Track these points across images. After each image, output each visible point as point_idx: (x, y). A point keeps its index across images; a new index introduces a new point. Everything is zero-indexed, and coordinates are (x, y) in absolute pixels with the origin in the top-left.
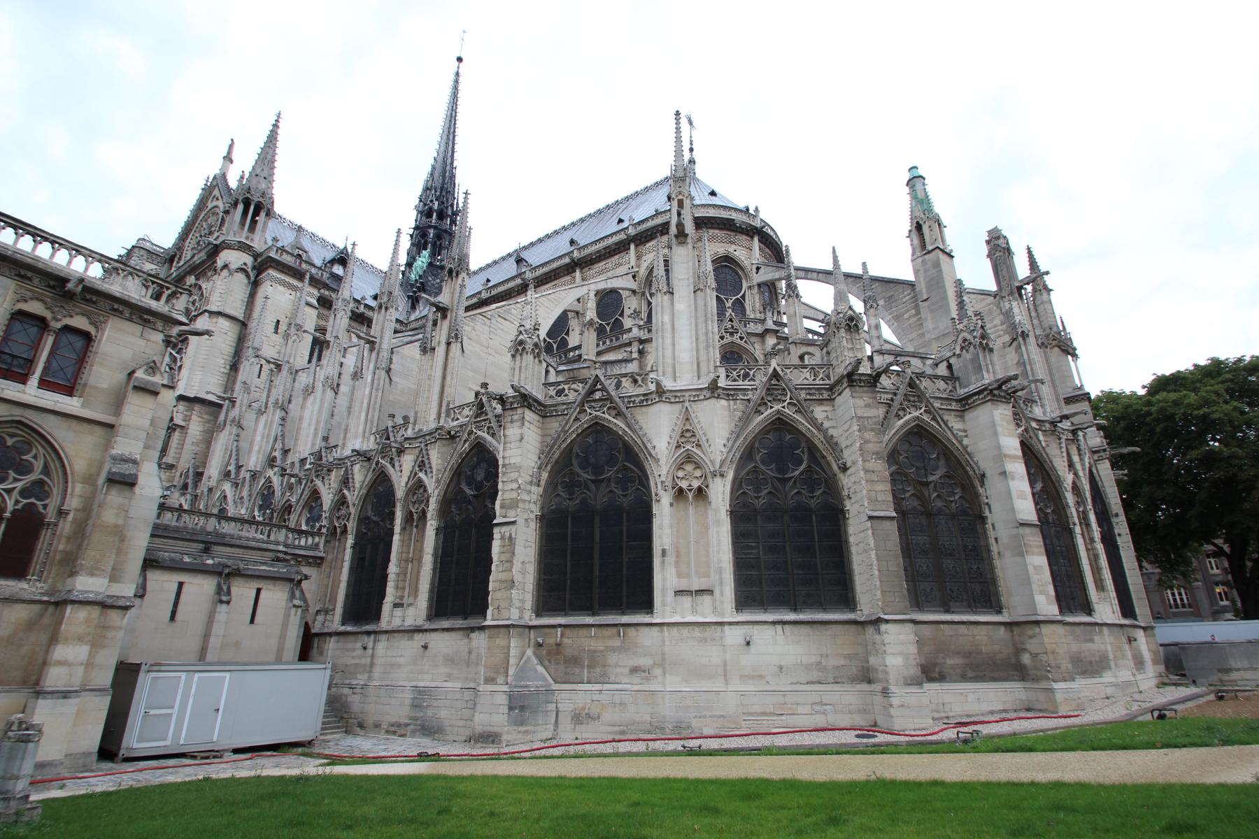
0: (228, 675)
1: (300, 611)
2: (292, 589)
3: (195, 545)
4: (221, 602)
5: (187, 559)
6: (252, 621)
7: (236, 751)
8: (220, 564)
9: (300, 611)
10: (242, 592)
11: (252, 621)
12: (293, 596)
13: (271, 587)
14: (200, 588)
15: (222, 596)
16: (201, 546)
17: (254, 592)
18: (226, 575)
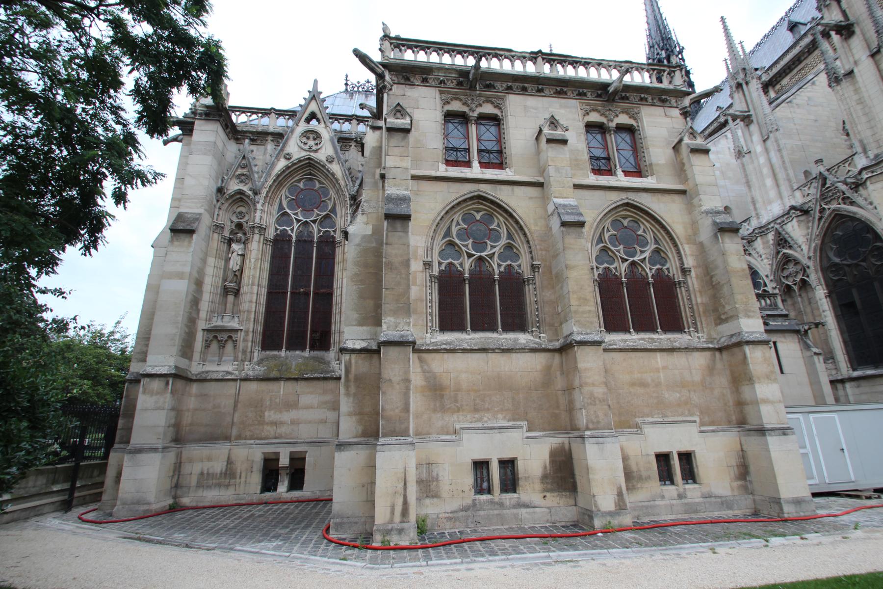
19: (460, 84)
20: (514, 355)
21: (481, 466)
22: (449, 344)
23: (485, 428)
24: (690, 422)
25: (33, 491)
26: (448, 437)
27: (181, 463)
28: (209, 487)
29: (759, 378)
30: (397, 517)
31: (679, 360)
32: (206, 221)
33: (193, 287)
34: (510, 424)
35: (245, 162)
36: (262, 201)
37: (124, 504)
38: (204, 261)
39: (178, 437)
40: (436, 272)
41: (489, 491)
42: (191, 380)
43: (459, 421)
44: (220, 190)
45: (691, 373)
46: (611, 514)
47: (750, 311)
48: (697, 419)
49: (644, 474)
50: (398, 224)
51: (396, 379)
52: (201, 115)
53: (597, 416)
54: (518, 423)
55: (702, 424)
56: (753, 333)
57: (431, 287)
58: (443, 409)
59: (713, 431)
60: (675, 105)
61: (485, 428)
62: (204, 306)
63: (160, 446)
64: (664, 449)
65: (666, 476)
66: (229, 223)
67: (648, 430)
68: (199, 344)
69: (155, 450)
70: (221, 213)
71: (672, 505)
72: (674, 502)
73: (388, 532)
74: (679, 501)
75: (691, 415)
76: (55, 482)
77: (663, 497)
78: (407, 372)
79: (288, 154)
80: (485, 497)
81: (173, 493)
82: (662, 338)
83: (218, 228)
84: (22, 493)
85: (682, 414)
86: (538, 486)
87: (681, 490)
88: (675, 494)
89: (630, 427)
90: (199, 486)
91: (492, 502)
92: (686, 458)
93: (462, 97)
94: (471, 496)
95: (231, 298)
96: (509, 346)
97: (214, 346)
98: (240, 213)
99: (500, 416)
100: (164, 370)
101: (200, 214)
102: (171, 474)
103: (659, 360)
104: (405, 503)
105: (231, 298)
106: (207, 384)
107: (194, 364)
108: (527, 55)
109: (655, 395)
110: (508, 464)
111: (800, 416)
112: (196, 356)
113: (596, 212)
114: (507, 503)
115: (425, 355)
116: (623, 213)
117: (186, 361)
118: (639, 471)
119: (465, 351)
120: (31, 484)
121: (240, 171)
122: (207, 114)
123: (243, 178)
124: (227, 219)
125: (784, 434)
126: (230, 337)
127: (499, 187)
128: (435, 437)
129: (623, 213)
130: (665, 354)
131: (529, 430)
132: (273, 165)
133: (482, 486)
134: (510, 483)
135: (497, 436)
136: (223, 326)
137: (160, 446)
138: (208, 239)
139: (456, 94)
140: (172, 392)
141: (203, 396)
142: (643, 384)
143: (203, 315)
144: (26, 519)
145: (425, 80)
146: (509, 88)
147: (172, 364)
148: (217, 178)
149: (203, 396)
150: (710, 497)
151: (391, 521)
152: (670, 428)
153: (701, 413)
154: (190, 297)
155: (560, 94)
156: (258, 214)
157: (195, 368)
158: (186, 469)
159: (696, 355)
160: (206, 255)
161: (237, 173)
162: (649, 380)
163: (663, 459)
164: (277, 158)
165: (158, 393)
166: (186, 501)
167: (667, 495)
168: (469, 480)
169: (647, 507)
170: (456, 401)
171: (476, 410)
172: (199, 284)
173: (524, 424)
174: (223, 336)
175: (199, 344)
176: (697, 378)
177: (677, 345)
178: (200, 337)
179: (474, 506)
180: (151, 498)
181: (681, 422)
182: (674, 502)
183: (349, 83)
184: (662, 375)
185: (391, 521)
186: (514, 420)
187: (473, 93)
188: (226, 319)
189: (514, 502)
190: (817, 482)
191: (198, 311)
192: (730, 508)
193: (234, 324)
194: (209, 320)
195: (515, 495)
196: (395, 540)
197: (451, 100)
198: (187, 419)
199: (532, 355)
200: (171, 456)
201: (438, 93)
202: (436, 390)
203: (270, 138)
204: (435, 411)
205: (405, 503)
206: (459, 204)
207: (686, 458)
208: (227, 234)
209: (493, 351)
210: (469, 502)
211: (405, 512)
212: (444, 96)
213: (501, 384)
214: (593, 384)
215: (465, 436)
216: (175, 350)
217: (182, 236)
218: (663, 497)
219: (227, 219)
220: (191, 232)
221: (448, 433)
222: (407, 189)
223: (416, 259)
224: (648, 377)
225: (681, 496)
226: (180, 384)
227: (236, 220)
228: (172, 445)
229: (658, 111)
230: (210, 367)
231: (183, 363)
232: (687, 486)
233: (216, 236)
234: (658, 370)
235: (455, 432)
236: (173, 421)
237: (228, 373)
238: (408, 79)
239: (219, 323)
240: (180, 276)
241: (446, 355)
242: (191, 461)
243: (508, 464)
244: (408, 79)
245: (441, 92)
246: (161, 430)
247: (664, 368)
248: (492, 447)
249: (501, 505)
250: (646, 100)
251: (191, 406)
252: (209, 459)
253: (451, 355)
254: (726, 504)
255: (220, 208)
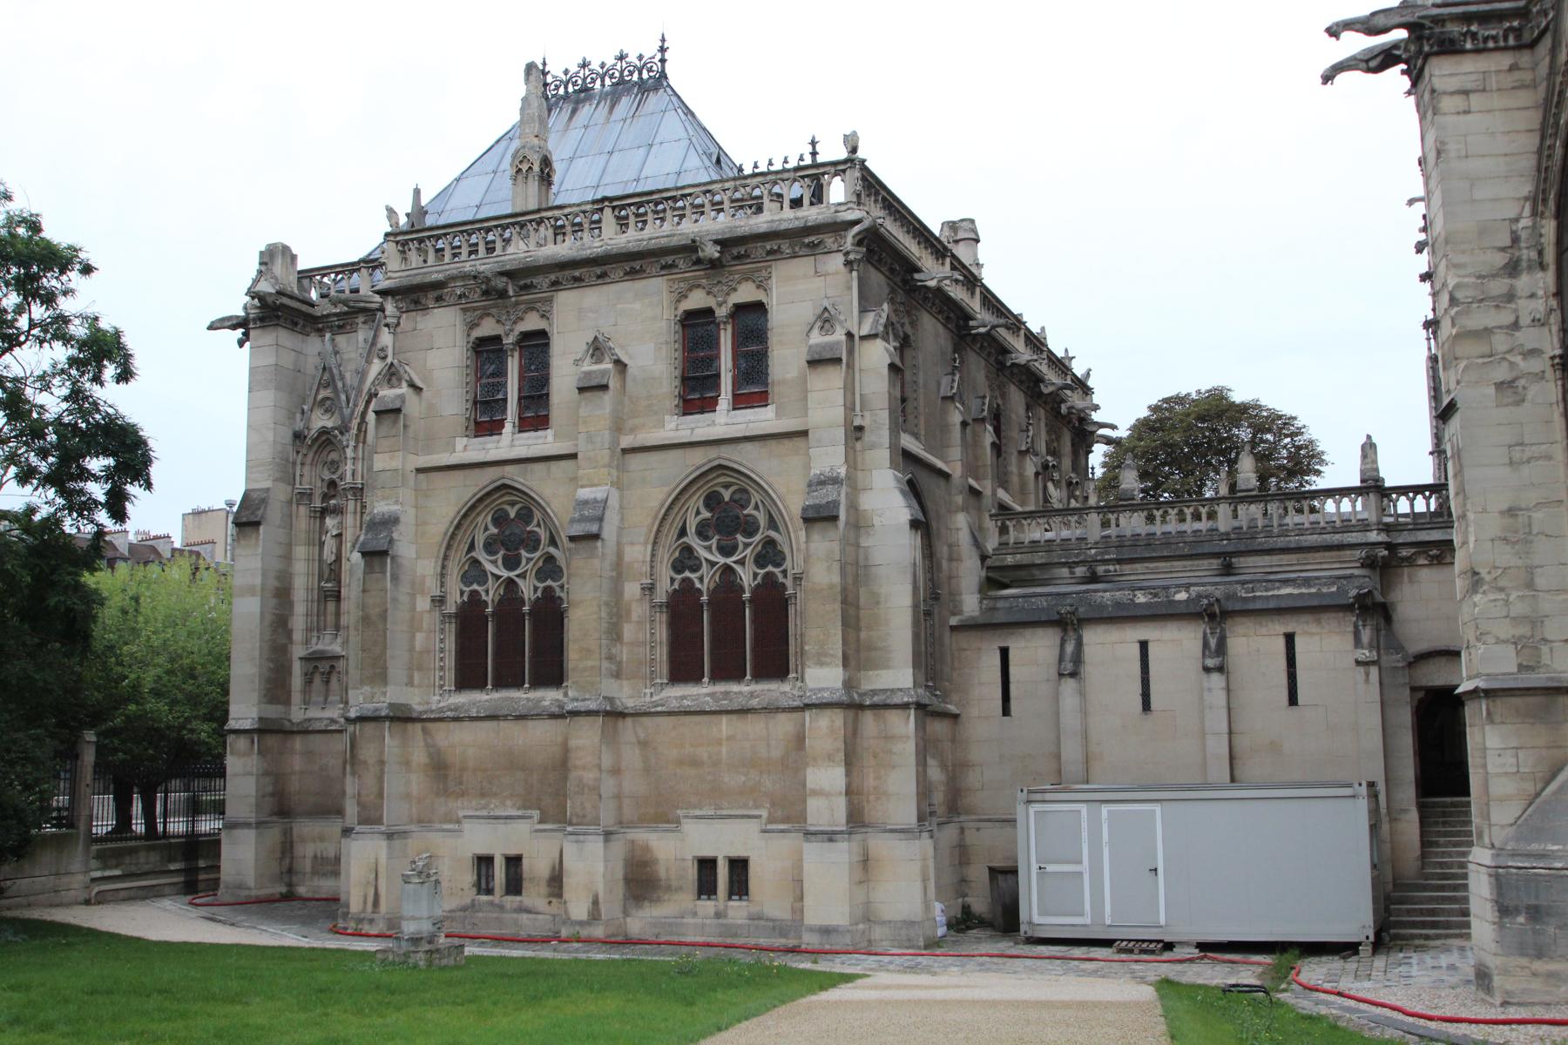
0: (1157, 808)
1: (1374, 671)
2: (1356, 627)
3: (1205, 563)
4: (1207, 670)
5: (1141, 598)
6: (1293, 700)
7: (1204, 947)
8: (1199, 596)
9: (1374, 671)
10: (1255, 646)
11: (1293, 700)
12: (1358, 643)
13: (1314, 628)
14: (1177, 645)
15: (1217, 660)
16: (1216, 563)
17: (1281, 643)
18: (1215, 616)
19: (486, 293)
20: (530, 723)
21: (484, 862)
22: (456, 709)
23: (489, 817)
24: (749, 817)
25: (146, 868)
26: (450, 826)
27: (292, 843)
28: (324, 875)
29: (815, 759)
30: (369, 908)
31: (755, 727)
32: (281, 493)
33: (273, 602)
34: (520, 813)
35: (328, 377)
36: (352, 443)
37: (227, 887)
38: (288, 557)
39: (281, 807)
40: (451, 608)
41: (489, 891)
42: (292, 732)
43: (462, 808)
44: (298, 436)
45: (769, 745)
46: (581, 923)
47: (826, 655)
48: (764, 813)
49: (674, 884)
50: (376, 561)
51: (371, 761)
52: (254, 320)
53: (583, 808)
54: (529, 812)
55: (771, 820)
56: (821, 690)
57: (442, 631)
58: (445, 792)
59: (782, 831)
60: (835, 247)
61: (489, 817)
62: (298, 623)
63: (253, 820)
64: (707, 853)
65: (706, 887)
66: (319, 484)
67: (689, 827)
68: (297, 681)
69: (247, 825)
70: (307, 468)
71: (703, 925)
72: (708, 921)
73: (360, 921)
74: (715, 921)
75: (756, 807)
76: (171, 860)
77: (695, 914)
78: (382, 752)
79: (382, 350)
80: (484, 898)
81: (286, 880)
82: (744, 690)
83: (306, 496)
84: (133, 869)
85: (745, 806)
86: (544, 889)
87: (722, 907)
88: (712, 911)
89: (668, 822)
90: (315, 873)
91: (491, 903)
92: (739, 866)
93: (493, 311)
94: (470, 894)
95: (331, 606)
96: (524, 712)
97: (317, 680)
98: (333, 462)
99: (509, 803)
100: (247, 725)
101: (268, 490)
102: (278, 855)
103: (724, 727)
104: (376, 894)
105: (331, 606)
106: (311, 737)
107: (294, 708)
108: (588, 207)
109: (709, 778)
110: (514, 862)
111: (1083, 808)
112: (296, 697)
113: (666, 489)
114: (508, 906)
115: (429, 725)
116: (722, 480)
117: (280, 708)
118: (668, 879)
119: (472, 719)
120: (142, 860)
121: (323, 394)
122: (262, 319)
123: (328, 403)
124: (312, 478)
125: (831, 840)
126: (332, 667)
127: (530, 466)
128: (437, 826)
129: (722, 480)
130: (734, 717)
131: (541, 822)
132: (362, 374)
133: (484, 885)
134: (515, 885)
135: (501, 827)
136: (323, 652)
137: (253, 820)
138: (288, 522)
139: (485, 308)
140: (260, 752)
141: (309, 754)
142: (695, 763)
143: (298, 636)
144: (144, 898)
145: (439, 299)
146: (555, 283)
147: (255, 715)
148: (291, 416)
149: (309, 754)
150: (760, 918)
151: (364, 910)
152: (718, 825)
153: (773, 804)
154: (269, 618)
155: (633, 274)
156: (349, 467)
157: (297, 714)
158: (299, 850)
159: (782, 717)
160: (290, 545)
161: (320, 397)
162: (705, 756)
163: (707, 866)
164: (369, 362)
165: (244, 755)
166: (302, 890)
167: (700, 913)
168: (469, 878)
169: (670, 925)
170: (461, 783)
171: (483, 795)
172: (283, 594)
173: (536, 814)
174: (324, 666)
175: (297, 681)
176: (777, 753)
177: (754, 703)
178: (297, 669)
179: (473, 907)
180: (251, 882)
181: (743, 817)
182: (708, 921)
183: (549, 79)
184: (724, 750)
185: (364, 910)
186: (525, 808)
187: (507, 302)
188: (328, 638)
189: (515, 905)
190: (1088, 921)
191: (289, 633)
192: (783, 934)
193: (336, 648)
194: (307, 642)
195: (518, 898)
196: (366, 928)
197: (481, 317)
198: (294, 784)
199: (553, 722)
200: (274, 834)
201: (459, 312)
202: (439, 768)
203: (361, 319)
204: (438, 794)
205: (376, 894)
206: (480, 500)
207: (739, 866)
208: (318, 504)
209: (505, 718)
210: (468, 901)
211: (376, 903)
212: (470, 317)
213: (513, 762)
214: (584, 768)
215: (466, 825)
216: (255, 697)
217: (248, 529)
218: (695, 914)
219: (312, 478)
220: (257, 524)
221: (450, 822)
222: (396, 502)
223: (423, 593)
224: (703, 753)
225: (718, 915)
226: (271, 740)
227: (327, 476)
228: (275, 818)
229: (803, 266)
230: (314, 713)
231: (273, 711)
232: (731, 903)
233: (303, 510)
234: (719, 742)
235: (458, 822)
236: (270, 789)
237: (333, 721)
238: (417, 302)
239: (320, 647)
240: (251, 591)
241: (452, 725)
242: (303, 840)
243: (514, 862)
244: (417, 302)
245: (465, 310)
246: (253, 800)
247: (730, 738)
248: (495, 840)
249: (501, 908)
250: (778, 251)
251: (297, 768)
252: (322, 839)
253: (457, 724)
254: (779, 928)
255: (302, 464)
